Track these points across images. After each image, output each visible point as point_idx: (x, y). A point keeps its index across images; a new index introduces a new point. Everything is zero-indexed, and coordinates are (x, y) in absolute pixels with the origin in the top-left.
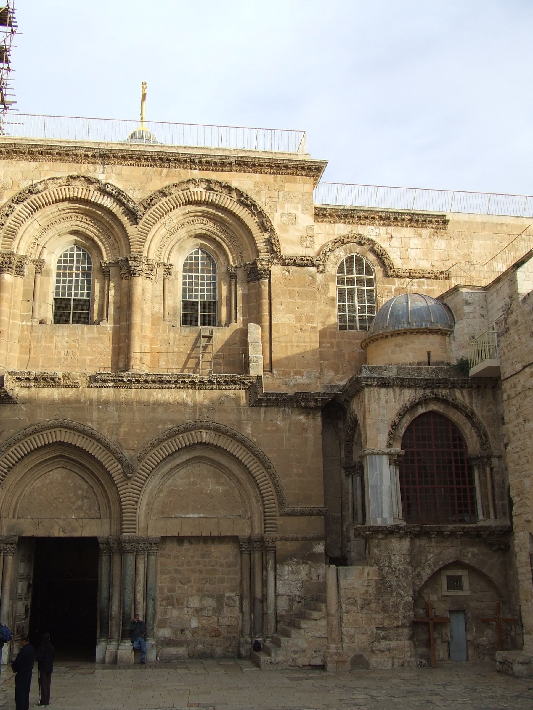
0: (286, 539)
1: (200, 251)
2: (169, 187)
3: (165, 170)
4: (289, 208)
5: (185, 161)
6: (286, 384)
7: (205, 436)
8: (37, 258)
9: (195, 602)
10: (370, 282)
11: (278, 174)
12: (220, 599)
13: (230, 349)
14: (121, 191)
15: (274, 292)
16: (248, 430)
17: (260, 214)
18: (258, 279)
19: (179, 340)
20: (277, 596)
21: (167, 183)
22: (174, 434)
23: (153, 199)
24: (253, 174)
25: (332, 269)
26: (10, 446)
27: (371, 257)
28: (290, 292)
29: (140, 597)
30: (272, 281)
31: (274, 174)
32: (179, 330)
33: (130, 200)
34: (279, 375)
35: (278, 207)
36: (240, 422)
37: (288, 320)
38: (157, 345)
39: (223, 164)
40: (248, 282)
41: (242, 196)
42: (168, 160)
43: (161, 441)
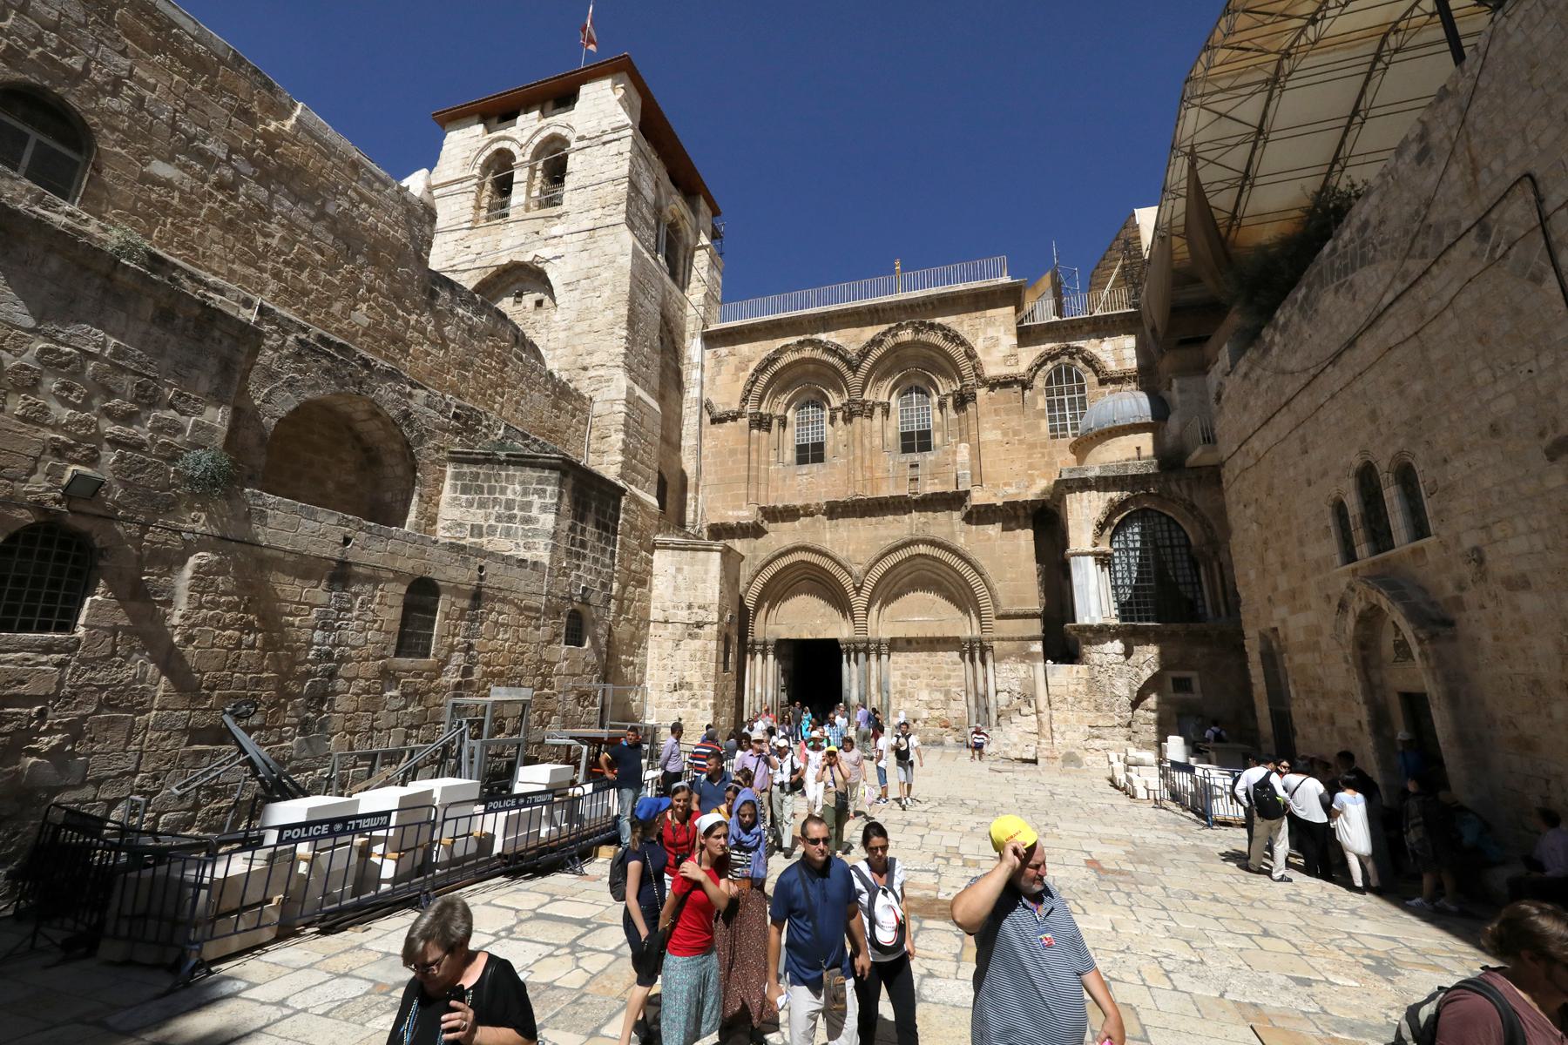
0: (1003, 639)
4: (991, 332)
5: (891, 309)
6: (995, 495)
7: (922, 549)
8: (780, 412)
9: (925, 695)
10: (1082, 389)
12: (947, 693)
16: (960, 542)
17: (963, 343)
20: (997, 692)
22: (896, 549)
25: (1040, 382)
26: (763, 567)
27: (1080, 364)
29: (873, 689)
33: (846, 352)
36: (953, 533)
43: (883, 556)
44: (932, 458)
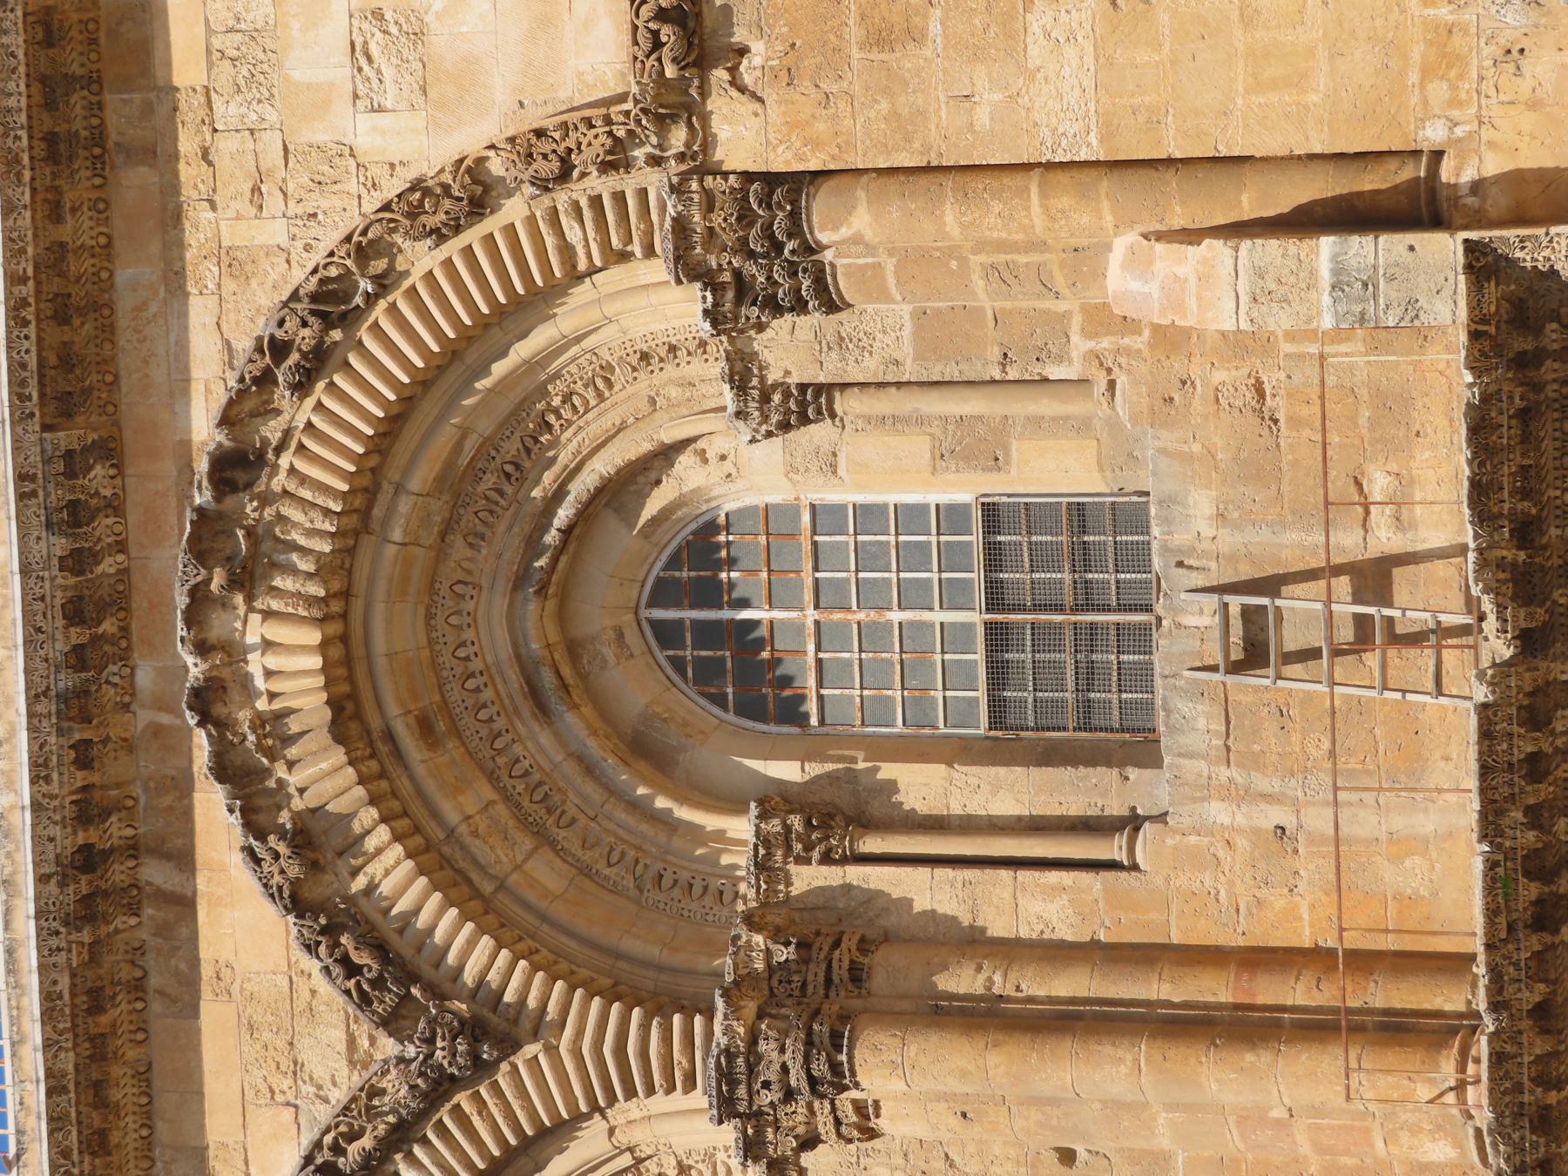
1: (659, 614)
2: (257, 861)
3: (155, 873)
5: (84, 756)
11: (98, 137)
13: (1295, 422)
14: (308, 1160)
15: (887, 150)
18: (809, 249)
19: (1255, 762)
21: (237, 859)
23: (345, 961)
24: (125, 303)
28: (880, 39)
30: (813, 166)
31: (99, 164)
32: (1182, 761)
34: (1455, 102)
35: (322, 136)
37: (1070, 52)
38: (1292, 914)
39: (73, 517)
40: (832, 304)
41: (265, 380)
42: (88, 860)
44: (1201, 504)
